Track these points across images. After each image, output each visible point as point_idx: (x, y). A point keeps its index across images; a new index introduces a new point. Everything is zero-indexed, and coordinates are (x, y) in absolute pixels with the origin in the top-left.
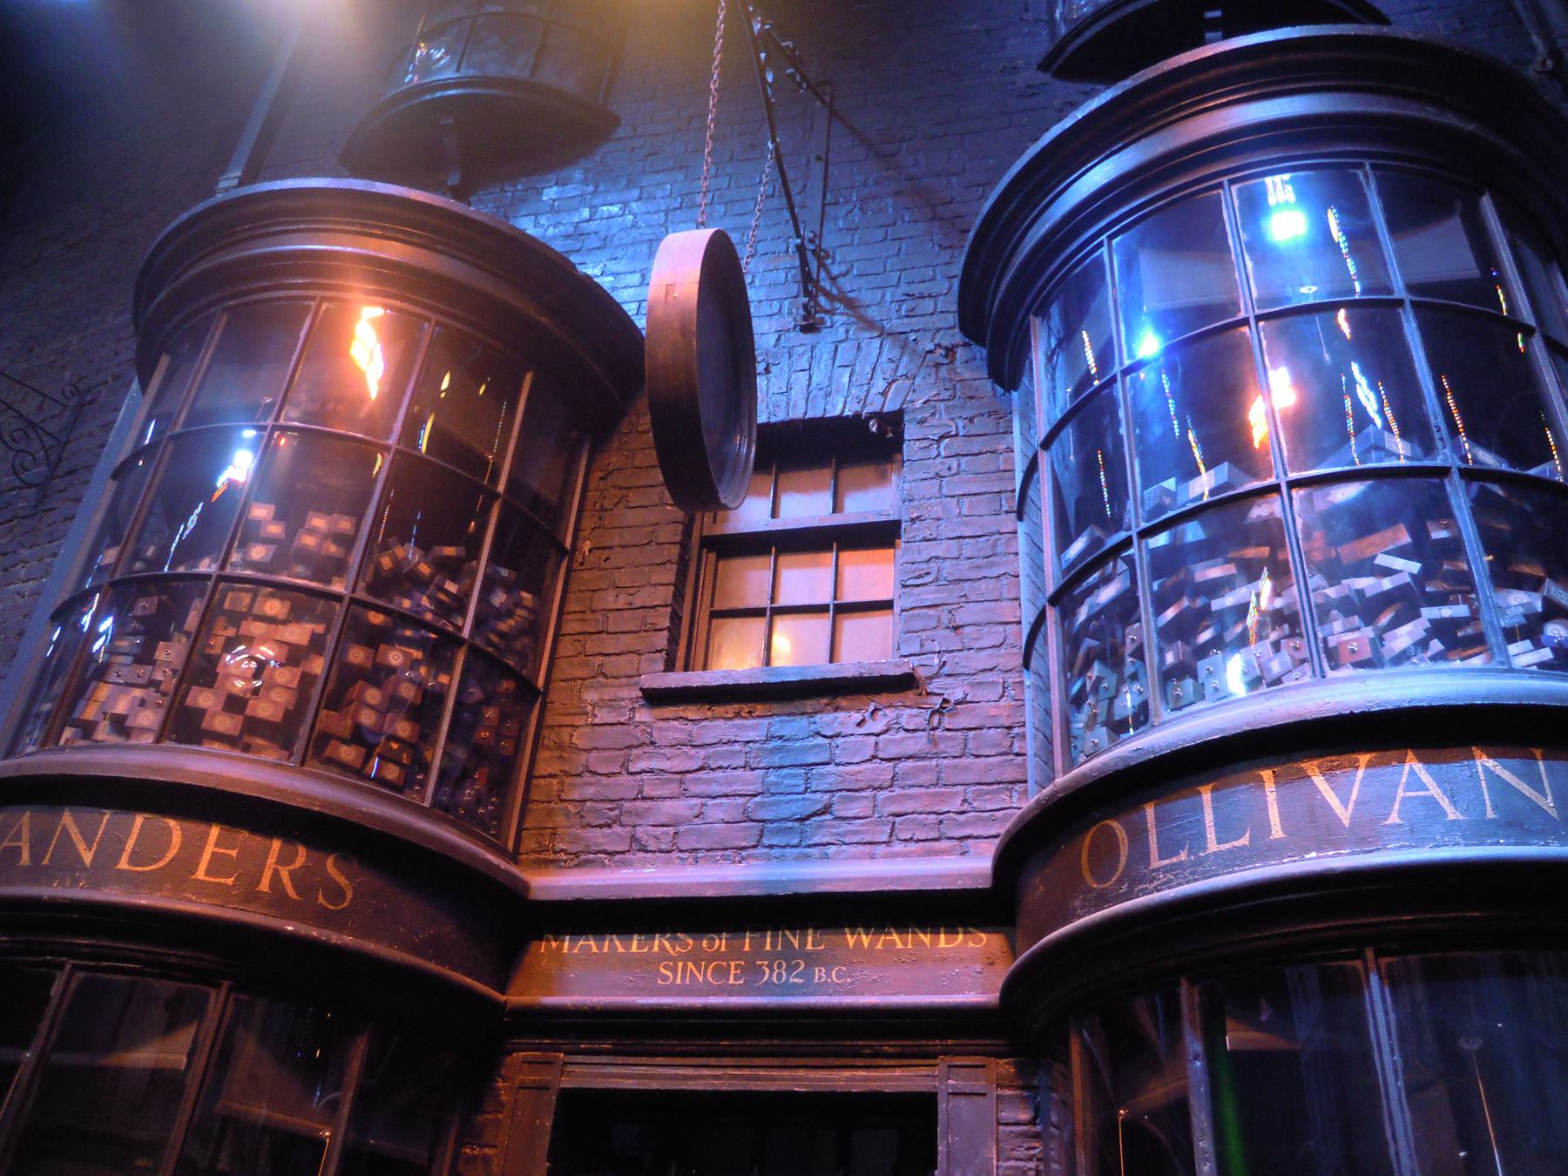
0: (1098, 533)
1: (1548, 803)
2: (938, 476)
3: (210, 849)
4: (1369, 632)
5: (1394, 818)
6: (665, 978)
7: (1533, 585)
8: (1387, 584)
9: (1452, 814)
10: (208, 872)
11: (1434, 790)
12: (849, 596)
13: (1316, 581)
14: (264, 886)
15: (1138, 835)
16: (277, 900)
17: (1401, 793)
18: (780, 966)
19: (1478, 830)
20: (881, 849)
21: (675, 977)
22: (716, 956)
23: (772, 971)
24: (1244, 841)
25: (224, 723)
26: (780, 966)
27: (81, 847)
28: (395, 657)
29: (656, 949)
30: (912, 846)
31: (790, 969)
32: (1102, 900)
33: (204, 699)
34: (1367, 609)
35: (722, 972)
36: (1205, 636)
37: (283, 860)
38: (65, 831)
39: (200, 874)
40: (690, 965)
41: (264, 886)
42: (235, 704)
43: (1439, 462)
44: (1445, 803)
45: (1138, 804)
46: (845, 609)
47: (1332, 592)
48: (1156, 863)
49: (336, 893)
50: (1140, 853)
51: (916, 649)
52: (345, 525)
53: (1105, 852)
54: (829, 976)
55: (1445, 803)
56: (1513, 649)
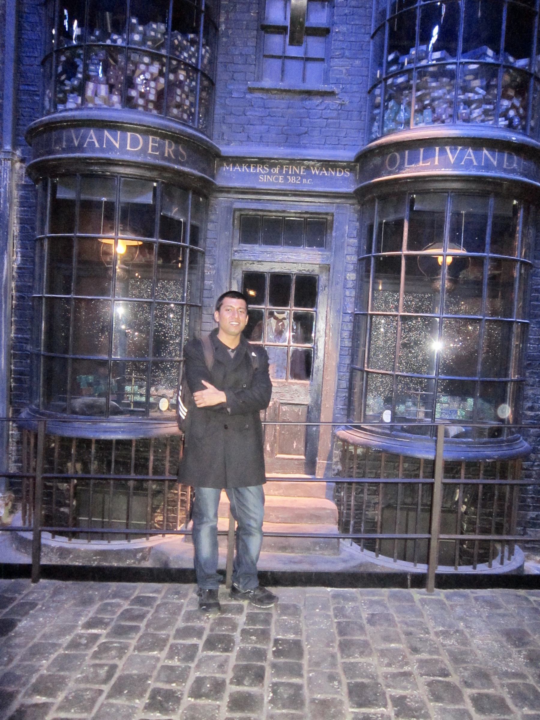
0: (398, 54)
1: (495, 163)
2: (346, 15)
3: (151, 144)
4: (468, 111)
5: (463, 163)
7: (509, 98)
8: (476, 97)
9: (475, 164)
10: (152, 151)
11: (473, 157)
12: (310, 55)
13: (459, 92)
14: (166, 155)
15: (403, 158)
16: (169, 159)
19: (479, 168)
20: (321, 146)
22: (275, 174)
24: (429, 164)
25: (141, 102)
27: (114, 142)
28: (182, 78)
30: (330, 146)
31: (296, 179)
32: (390, 173)
33: (134, 93)
34: (468, 103)
35: (277, 179)
36: (427, 102)
37: (170, 146)
38: (107, 137)
39: (150, 151)
41: (166, 155)
42: (142, 95)
43: (499, 62)
44: (474, 161)
45: (404, 150)
46: (308, 59)
47: (462, 97)
48: (406, 166)
50: (402, 163)
51: (335, 82)
52: (162, 27)
53: (393, 162)
55: (474, 161)
56: (500, 119)
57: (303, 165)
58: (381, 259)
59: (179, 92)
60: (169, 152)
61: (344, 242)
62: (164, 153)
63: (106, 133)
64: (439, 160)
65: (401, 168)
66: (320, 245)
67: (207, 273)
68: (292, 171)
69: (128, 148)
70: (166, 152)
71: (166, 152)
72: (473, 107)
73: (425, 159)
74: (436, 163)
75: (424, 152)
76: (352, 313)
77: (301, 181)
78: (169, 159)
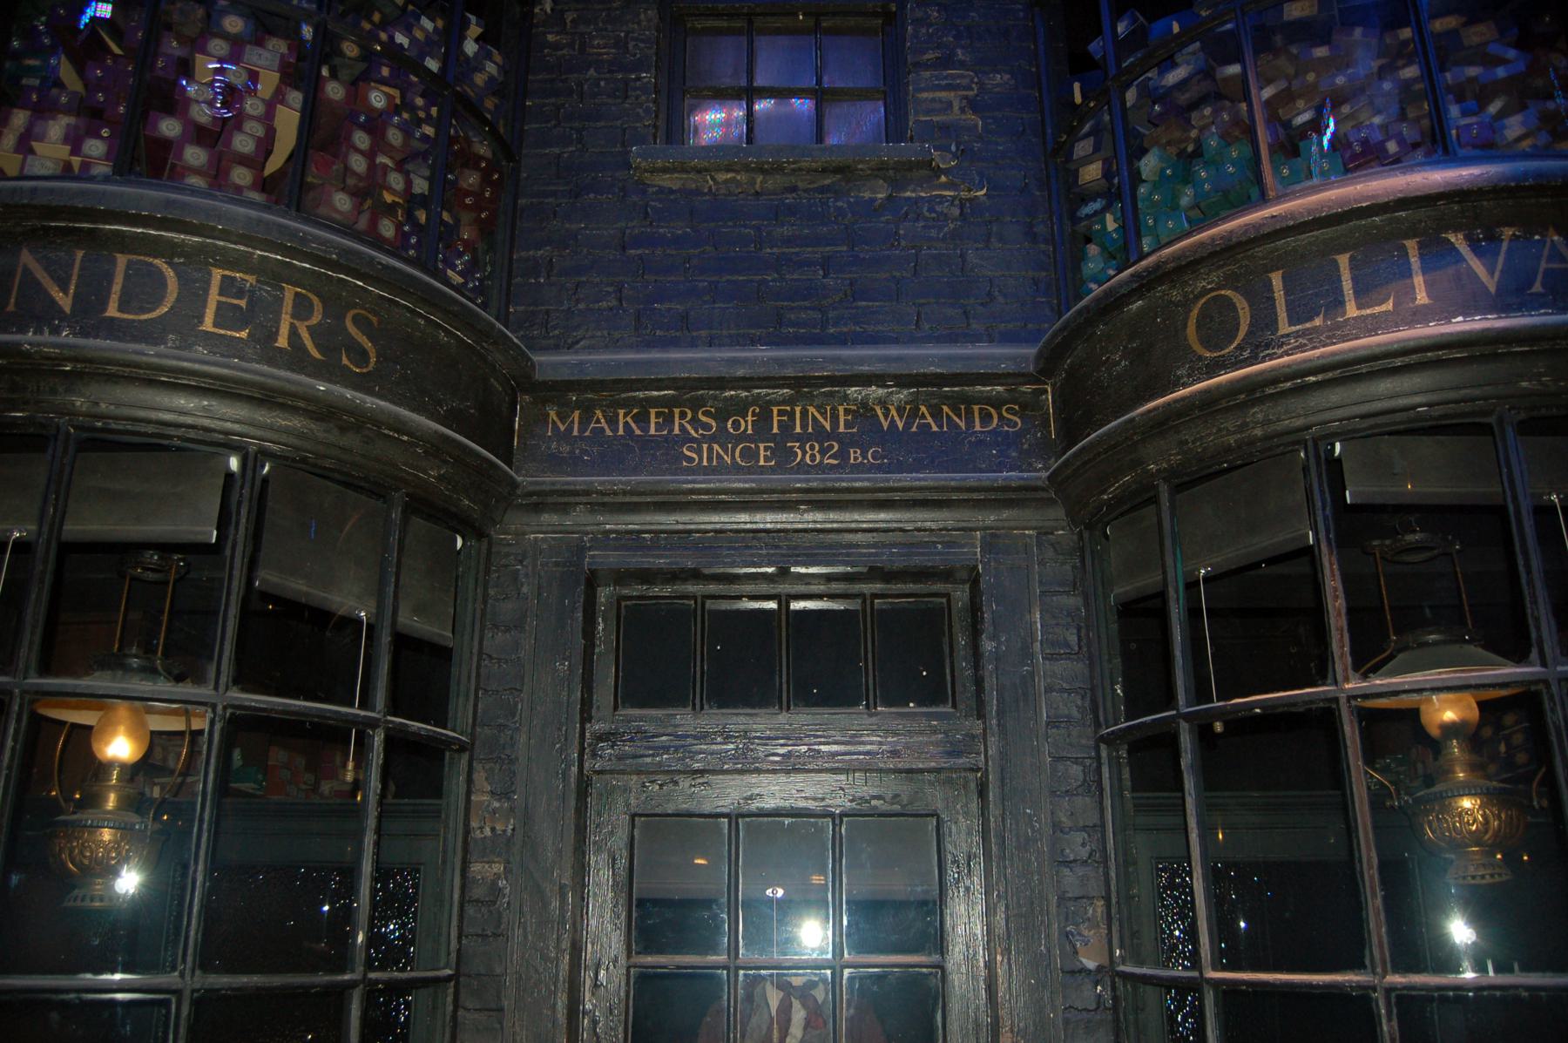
5: (1537, 287)
6: (691, 460)
8: (1501, 72)
10: (215, 325)
14: (282, 342)
16: (296, 358)
17: (1543, 265)
18: (812, 448)
21: (701, 459)
23: (804, 453)
24: (1389, 306)
25: (195, 155)
26: (812, 448)
29: (677, 431)
31: (823, 452)
37: (302, 308)
39: (208, 325)
40: (716, 447)
41: (282, 342)
48: (1284, 328)
49: (361, 356)
50: (1264, 320)
53: (1218, 325)
54: (865, 457)
57: (846, 398)
58: (1218, 727)
59: (361, 139)
60: (294, 333)
61: (1032, 674)
62: (273, 336)
63: (27, 258)
64: (1429, 286)
65: (1261, 341)
66: (933, 693)
67: (482, 831)
68: (804, 426)
69: (112, 311)
70: (284, 330)
71: (284, 330)
72: (1493, 108)
73: (1364, 293)
74: (1422, 298)
75: (1354, 265)
76: (1100, 969)
77: (842, 455)
78: (296, 358)
